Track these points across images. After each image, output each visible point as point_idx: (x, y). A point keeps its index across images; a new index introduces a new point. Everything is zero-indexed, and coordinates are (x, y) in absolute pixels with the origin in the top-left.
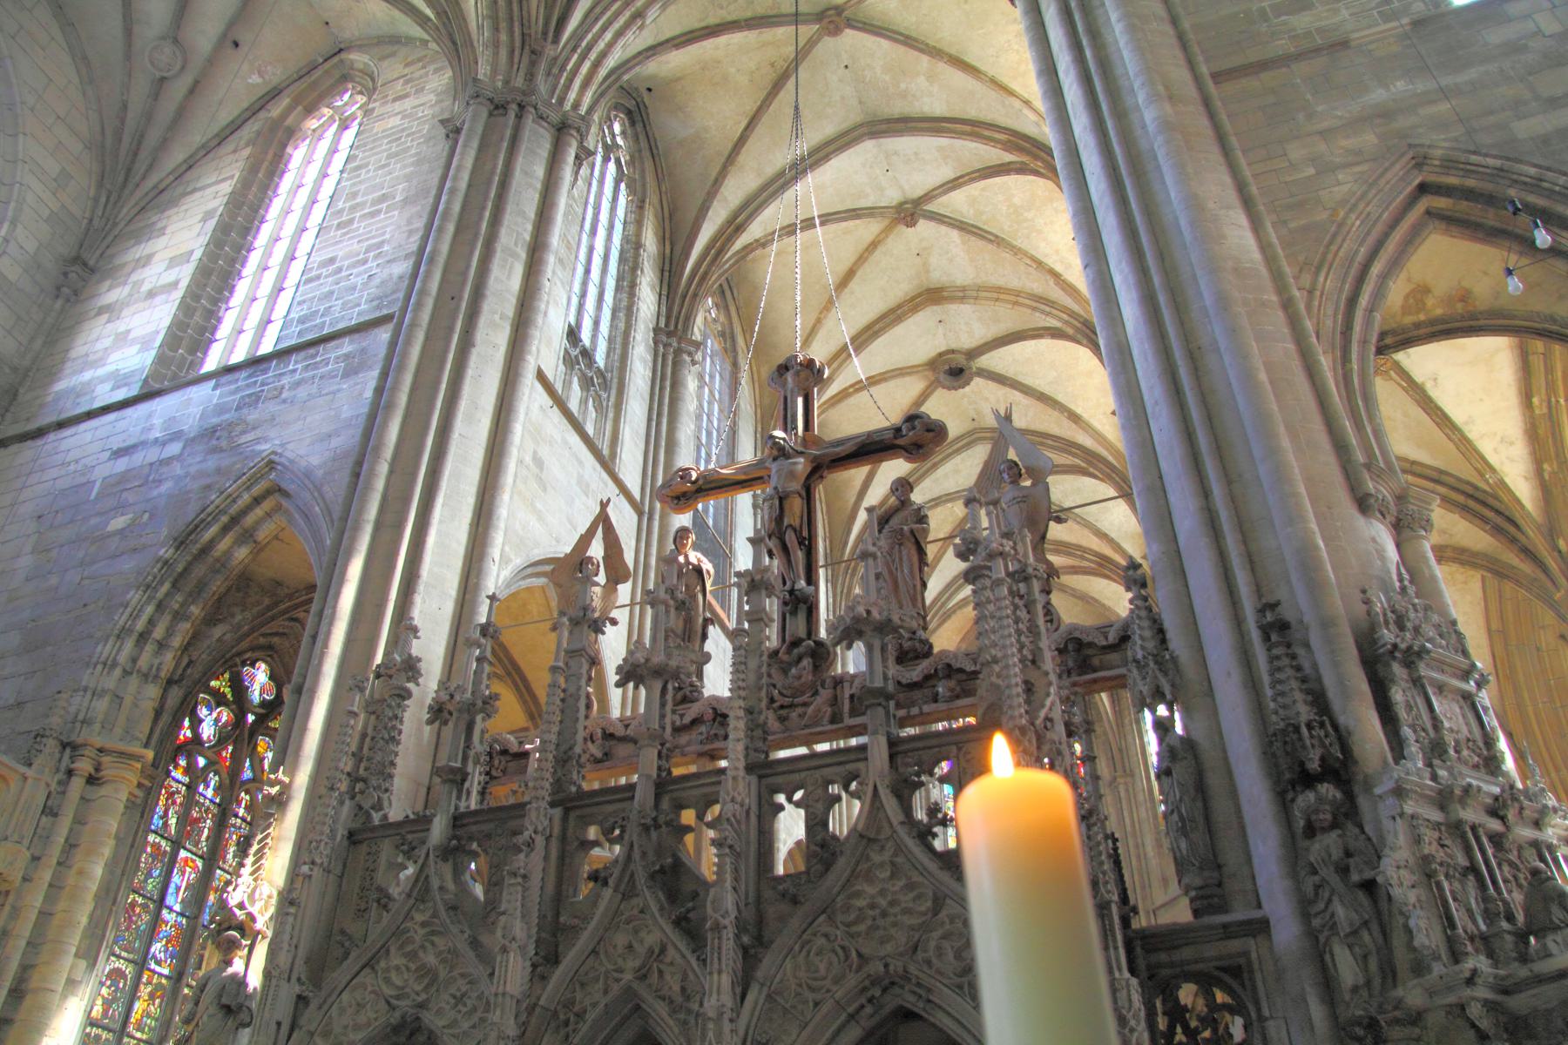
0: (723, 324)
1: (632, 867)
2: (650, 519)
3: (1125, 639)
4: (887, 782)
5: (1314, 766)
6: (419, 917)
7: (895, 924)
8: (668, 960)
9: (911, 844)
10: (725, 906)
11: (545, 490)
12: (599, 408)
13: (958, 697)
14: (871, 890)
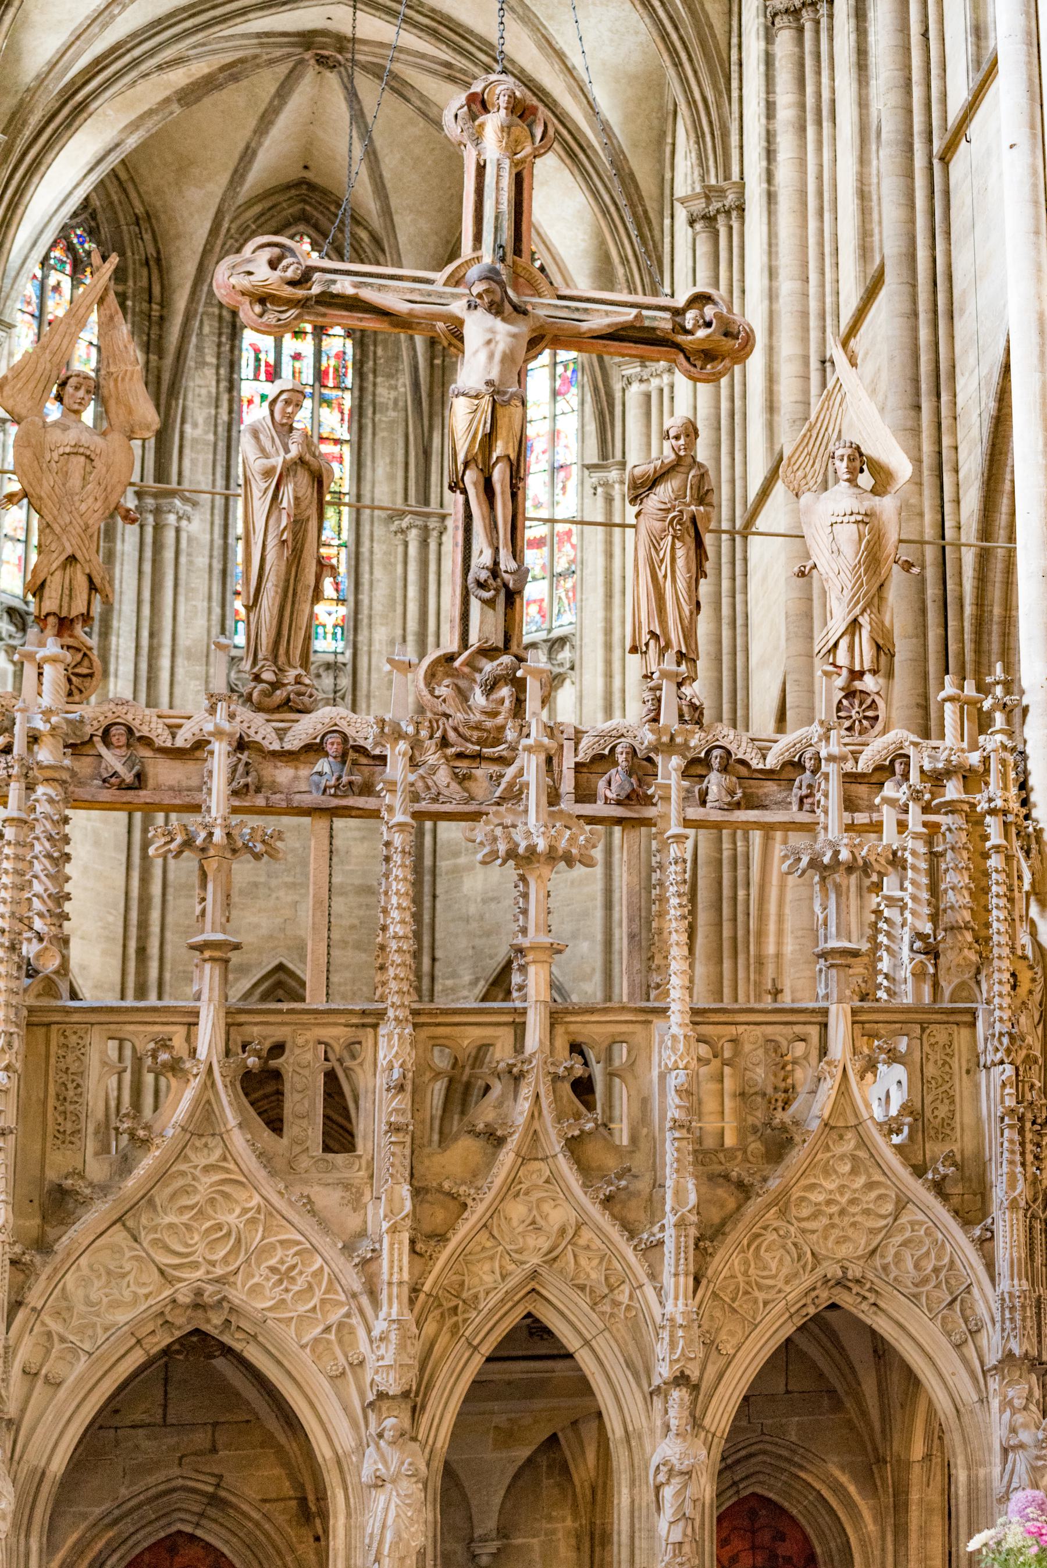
13: (738, 806)
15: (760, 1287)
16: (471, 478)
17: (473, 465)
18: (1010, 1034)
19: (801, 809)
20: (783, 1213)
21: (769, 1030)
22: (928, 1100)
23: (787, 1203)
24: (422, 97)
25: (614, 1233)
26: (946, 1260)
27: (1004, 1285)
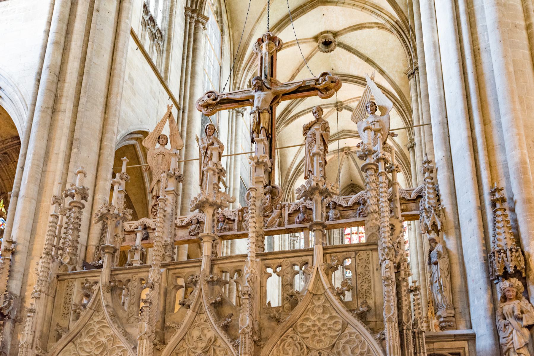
0: (216, 7)
1: (201, 300)
3: (420, 196)
4: (323, 268)
5: (511, 270)
6: (96, 319)
7: (324, 334)
8: (218, 344)
9: (334, 298)
10: (245, 321)
11: (135, 95)
12: (159, 51)
14: (313, 318)
17: (255, 133)
19: (359, 217)
20: (295, 330)
23: (296, 326)
26: (366, 349)
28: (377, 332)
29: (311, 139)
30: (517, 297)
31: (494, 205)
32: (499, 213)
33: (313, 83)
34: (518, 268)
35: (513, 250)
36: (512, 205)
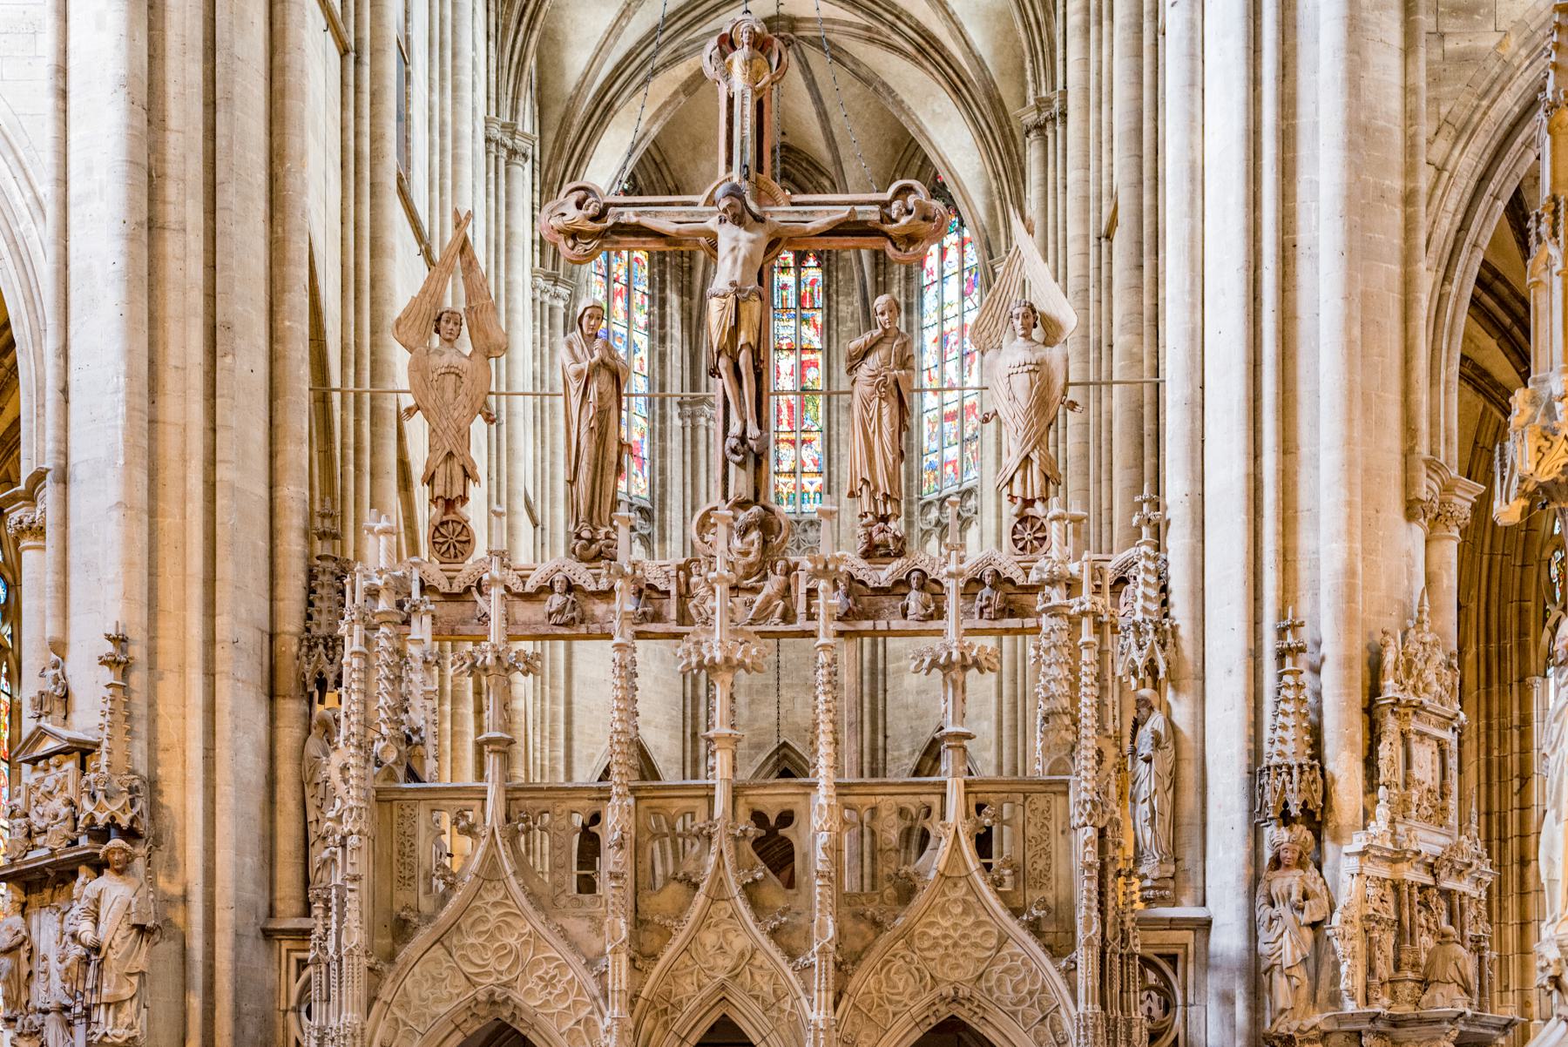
2: (358, 61)
15: (890, 1002)
16: (723, 363)
18: (1093, 802)
21: (900, 799)
22: (1029, 855)
24: (855, 61)
25: (778, 956)
26: (1039, 985)
27: (1081, 1006)
28: (1062, 956)
29: (868, 389)
30: (1301, 864)
31: (1281, 656)
32: (1288, 679)
33: (872, 215)
34: (1310, 807)
35: (1306, 768)
36: (1315, 659)
